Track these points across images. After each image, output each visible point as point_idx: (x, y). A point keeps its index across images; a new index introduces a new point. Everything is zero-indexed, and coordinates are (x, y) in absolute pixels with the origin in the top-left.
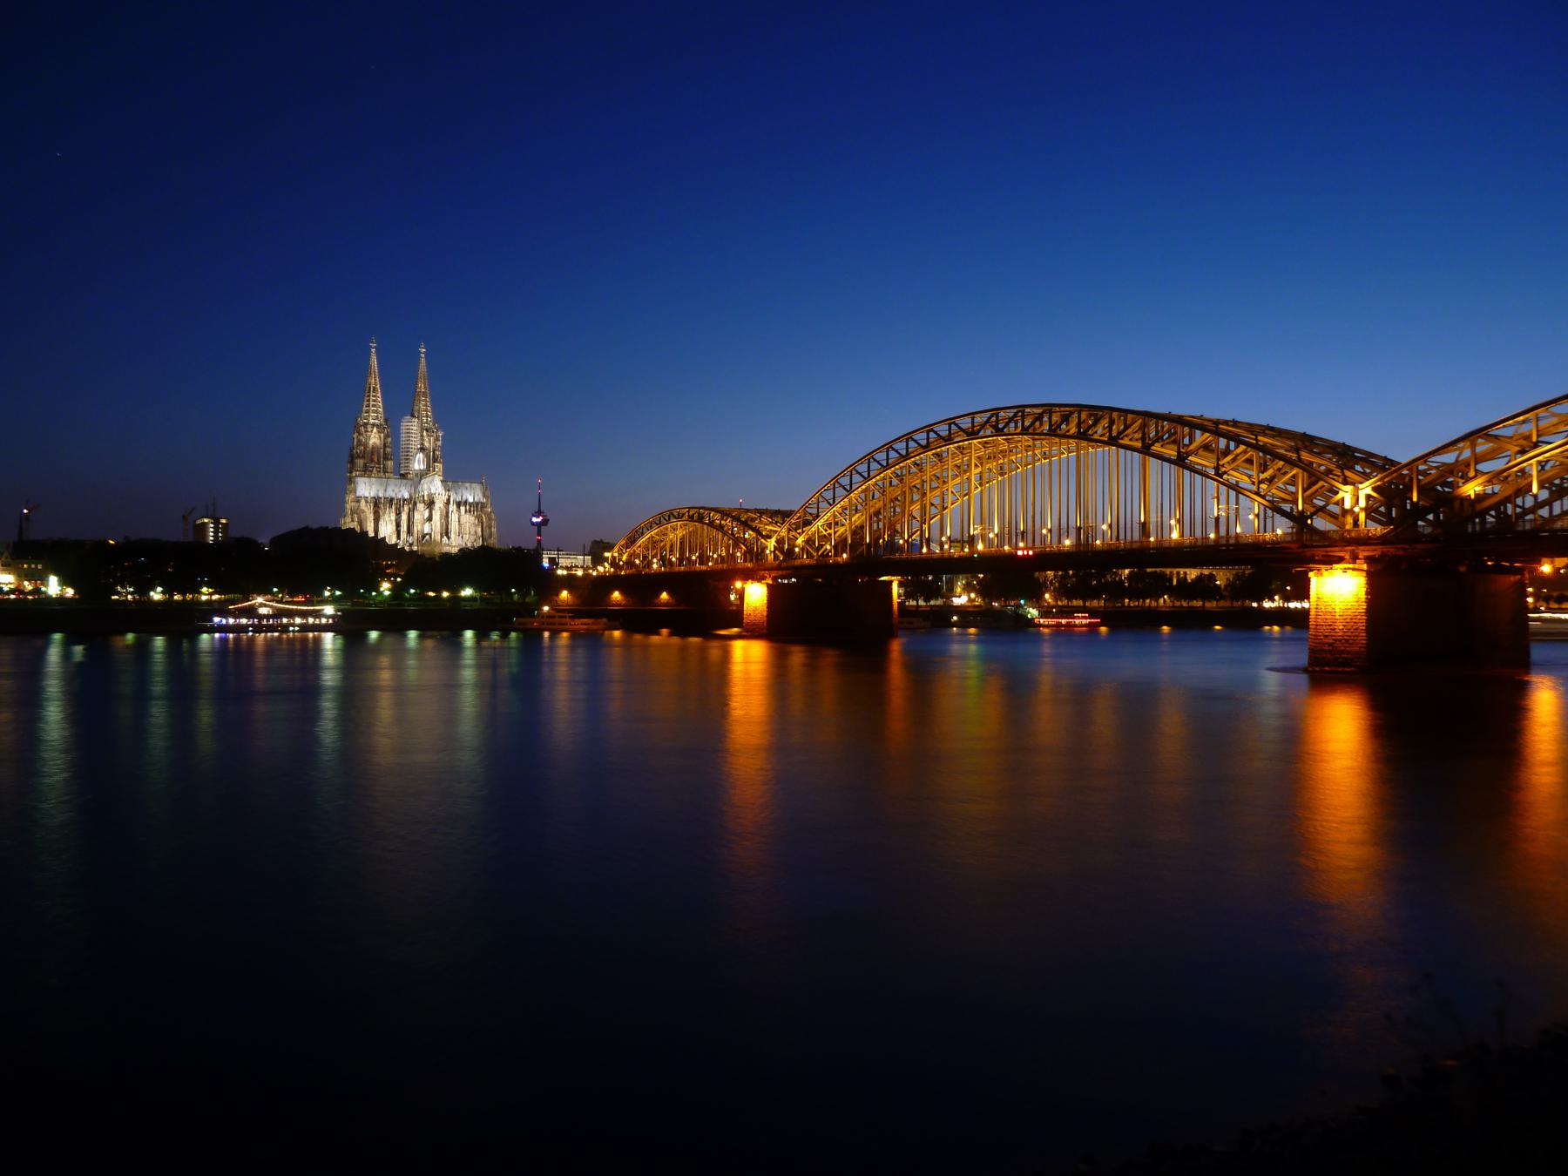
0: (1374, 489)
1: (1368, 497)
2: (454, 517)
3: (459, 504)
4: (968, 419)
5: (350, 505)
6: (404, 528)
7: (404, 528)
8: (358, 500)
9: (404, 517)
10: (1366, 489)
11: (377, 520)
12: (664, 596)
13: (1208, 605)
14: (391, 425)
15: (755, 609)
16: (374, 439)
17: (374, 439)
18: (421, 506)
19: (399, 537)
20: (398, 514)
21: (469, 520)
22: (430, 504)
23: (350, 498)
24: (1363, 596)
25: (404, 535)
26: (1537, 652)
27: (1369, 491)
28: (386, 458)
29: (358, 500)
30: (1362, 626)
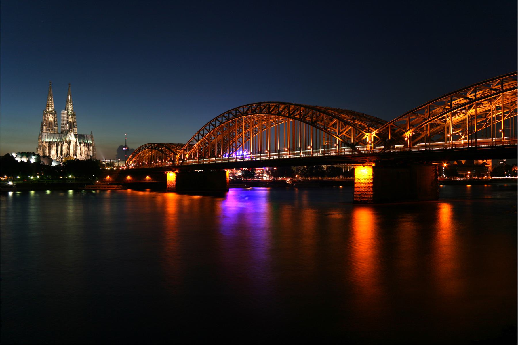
0: (376, 134)
1: (374, 137)
2: (78, 148)
3: (80, 143)
4: (242, 109)
6: (59, 152)
7: (59, 152)
9: (59, 148)
10: (374, 134)
13: (333, 179)
15: (171, 182)
16: (51, 118)
18: (66, 144)
19: (57, 156)
20: (57, 147)
21: (84, 149)
22: (69, 143)
24: (371, 176)
25: (59, 155)
26: (207, 199)
27: (374, 135)
30: (371, 187)
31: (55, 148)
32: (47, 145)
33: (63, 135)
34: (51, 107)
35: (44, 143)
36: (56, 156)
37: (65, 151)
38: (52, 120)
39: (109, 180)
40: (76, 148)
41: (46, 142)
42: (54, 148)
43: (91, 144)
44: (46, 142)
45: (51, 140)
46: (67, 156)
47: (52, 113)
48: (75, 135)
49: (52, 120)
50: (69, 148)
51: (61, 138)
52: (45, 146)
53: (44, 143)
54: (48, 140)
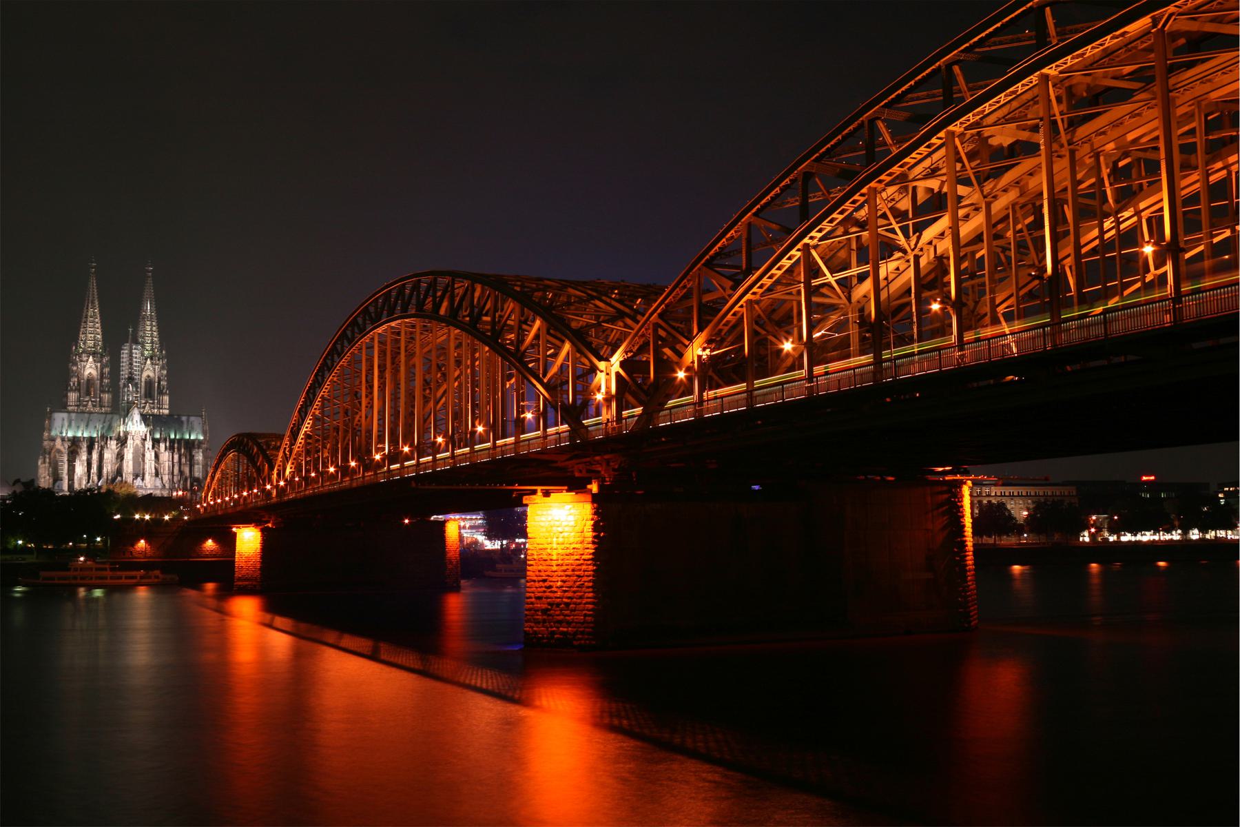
1: (618, 374)
5: (46, 443)
6: (94, 469)
7: (94, 469)
8: (53, 440)
9: (95, 456)
12: (210, 543)
15: (248, 559)
17: (90, 368)
18: (113, 444)
22: (122, 441)
23: (46, 434)
24: (589, 535)
28: (103, 392)
29: (53, 440)
30: (587, 581)
31: (84, 457)
33: (116, 417)
34: (92, 333)
35: (59, 441)
36: (84, 482)
37: (108, 468)
38: (94, 373)
39: (143, 553)
41: (63, 439)
43: (200, 442)
45: (79, 434)
46: (114, 479)
47: (94, 354)
49: (94, 373)
50: (120, 457)
51: (110, 428)
52: (59, 451)
53: (59, 441)
54: (70, 434)
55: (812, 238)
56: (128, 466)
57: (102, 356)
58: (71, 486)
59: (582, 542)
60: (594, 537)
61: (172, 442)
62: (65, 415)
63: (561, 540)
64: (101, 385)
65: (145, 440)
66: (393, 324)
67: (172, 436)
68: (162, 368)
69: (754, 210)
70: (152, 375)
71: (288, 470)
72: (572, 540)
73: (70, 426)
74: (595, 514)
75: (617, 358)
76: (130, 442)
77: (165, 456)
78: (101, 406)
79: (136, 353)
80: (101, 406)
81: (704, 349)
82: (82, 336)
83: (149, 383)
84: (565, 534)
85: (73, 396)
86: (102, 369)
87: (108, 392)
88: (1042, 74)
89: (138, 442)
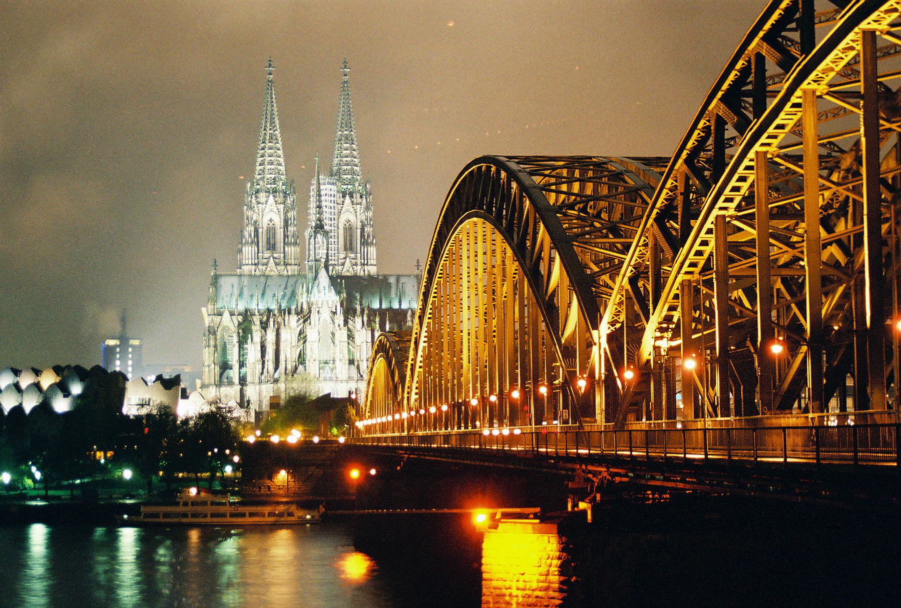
11: (242, 343)
14: (294, 189)
18: (293, 318)
22: (305, 316)
24: (555, 578)
32: (230, 323)
35: (226, 315)
40: (333, 334)
42: (257, 335)
44: (232, 314)
45: (253, 306)
47: (275, 191)
48: (335, 281)
50: (302, 336)
51: (293, 294)
52: (226, 329)
53: (226, 315)
54: (241, 307)
55: (721, 209)
56: (314, 352)
57: (286, 195)
58: (243, 381)
59: (547, 589)
60: (561, 583)
61: (372, 313)
62: (235, 280)
63: (521, 585)
64: (286, 236)
65: (335, 313)
66: (475, 219)
67: (376, 305)
68: (367, 208)
69: (684, 155)
70: (352, 218)
71: (414, 397)
72: (534, 585)
73: (241, 294)
74: (562, 550)
75: (605, 328)
76: (314, 317)
77: (363, 336)
78: (286, 264)
79: (329, 189)
80: (286, 264)
81: (657, 338)
82: (258, 168)
83: (349, 230)
84: (525, 577)
85: (248, 251)
86: (286, 214)
87: (295, 244)
88: (864, 32)
89: (326, 315)
